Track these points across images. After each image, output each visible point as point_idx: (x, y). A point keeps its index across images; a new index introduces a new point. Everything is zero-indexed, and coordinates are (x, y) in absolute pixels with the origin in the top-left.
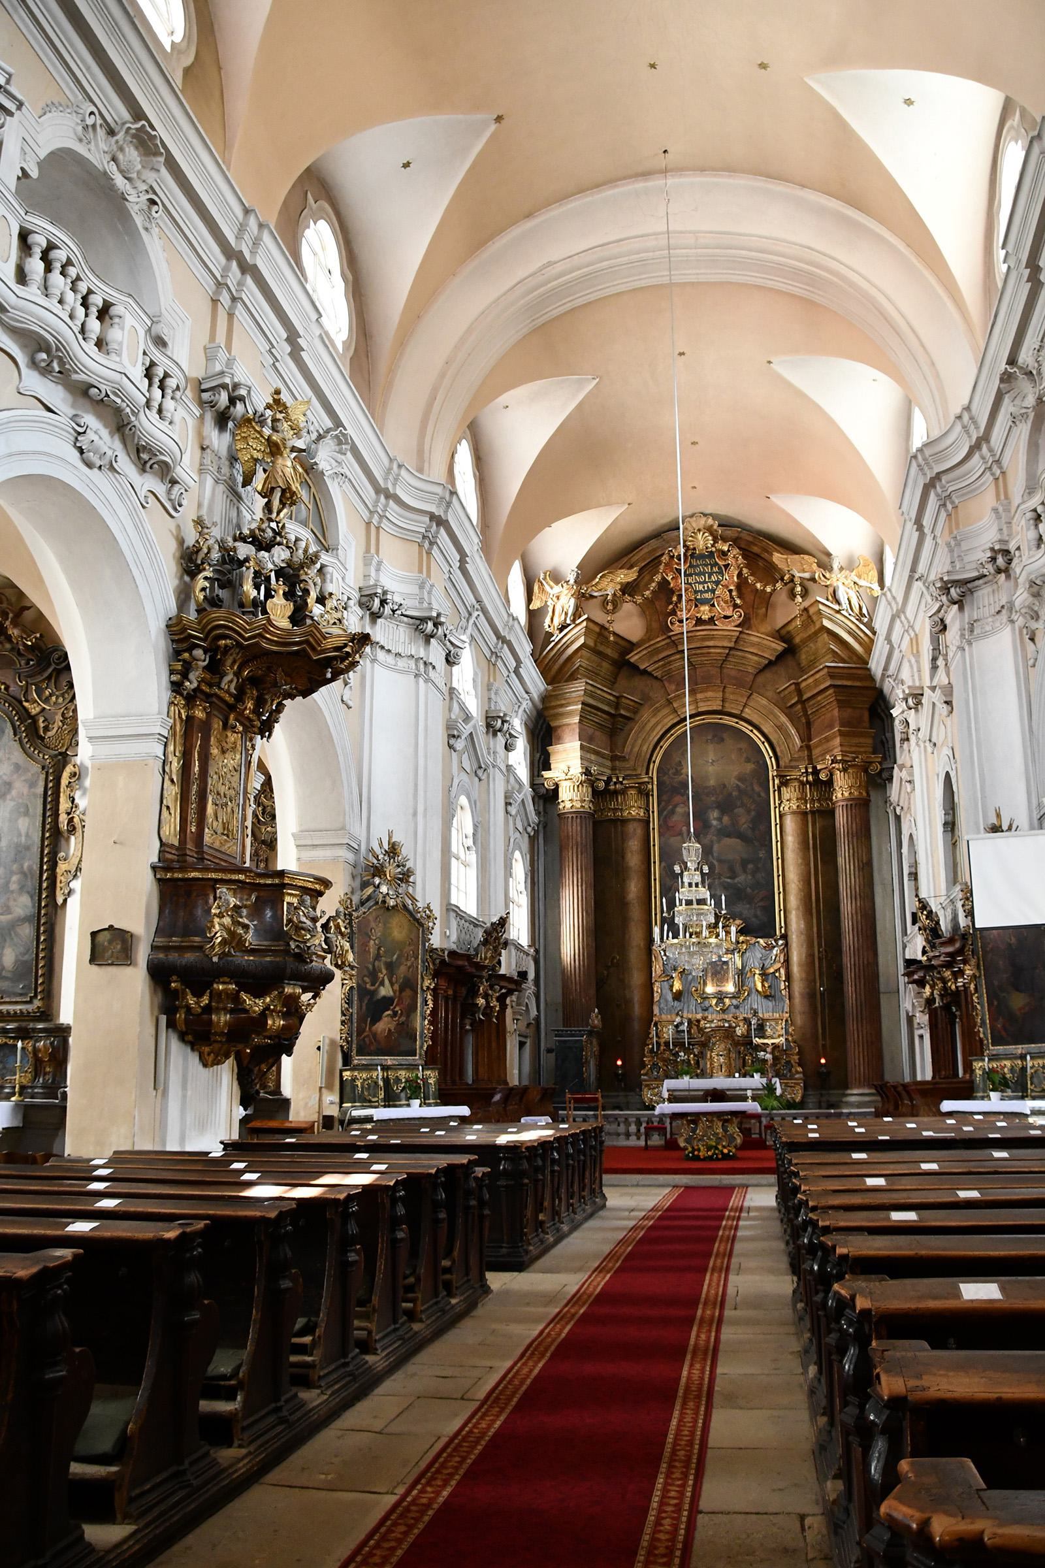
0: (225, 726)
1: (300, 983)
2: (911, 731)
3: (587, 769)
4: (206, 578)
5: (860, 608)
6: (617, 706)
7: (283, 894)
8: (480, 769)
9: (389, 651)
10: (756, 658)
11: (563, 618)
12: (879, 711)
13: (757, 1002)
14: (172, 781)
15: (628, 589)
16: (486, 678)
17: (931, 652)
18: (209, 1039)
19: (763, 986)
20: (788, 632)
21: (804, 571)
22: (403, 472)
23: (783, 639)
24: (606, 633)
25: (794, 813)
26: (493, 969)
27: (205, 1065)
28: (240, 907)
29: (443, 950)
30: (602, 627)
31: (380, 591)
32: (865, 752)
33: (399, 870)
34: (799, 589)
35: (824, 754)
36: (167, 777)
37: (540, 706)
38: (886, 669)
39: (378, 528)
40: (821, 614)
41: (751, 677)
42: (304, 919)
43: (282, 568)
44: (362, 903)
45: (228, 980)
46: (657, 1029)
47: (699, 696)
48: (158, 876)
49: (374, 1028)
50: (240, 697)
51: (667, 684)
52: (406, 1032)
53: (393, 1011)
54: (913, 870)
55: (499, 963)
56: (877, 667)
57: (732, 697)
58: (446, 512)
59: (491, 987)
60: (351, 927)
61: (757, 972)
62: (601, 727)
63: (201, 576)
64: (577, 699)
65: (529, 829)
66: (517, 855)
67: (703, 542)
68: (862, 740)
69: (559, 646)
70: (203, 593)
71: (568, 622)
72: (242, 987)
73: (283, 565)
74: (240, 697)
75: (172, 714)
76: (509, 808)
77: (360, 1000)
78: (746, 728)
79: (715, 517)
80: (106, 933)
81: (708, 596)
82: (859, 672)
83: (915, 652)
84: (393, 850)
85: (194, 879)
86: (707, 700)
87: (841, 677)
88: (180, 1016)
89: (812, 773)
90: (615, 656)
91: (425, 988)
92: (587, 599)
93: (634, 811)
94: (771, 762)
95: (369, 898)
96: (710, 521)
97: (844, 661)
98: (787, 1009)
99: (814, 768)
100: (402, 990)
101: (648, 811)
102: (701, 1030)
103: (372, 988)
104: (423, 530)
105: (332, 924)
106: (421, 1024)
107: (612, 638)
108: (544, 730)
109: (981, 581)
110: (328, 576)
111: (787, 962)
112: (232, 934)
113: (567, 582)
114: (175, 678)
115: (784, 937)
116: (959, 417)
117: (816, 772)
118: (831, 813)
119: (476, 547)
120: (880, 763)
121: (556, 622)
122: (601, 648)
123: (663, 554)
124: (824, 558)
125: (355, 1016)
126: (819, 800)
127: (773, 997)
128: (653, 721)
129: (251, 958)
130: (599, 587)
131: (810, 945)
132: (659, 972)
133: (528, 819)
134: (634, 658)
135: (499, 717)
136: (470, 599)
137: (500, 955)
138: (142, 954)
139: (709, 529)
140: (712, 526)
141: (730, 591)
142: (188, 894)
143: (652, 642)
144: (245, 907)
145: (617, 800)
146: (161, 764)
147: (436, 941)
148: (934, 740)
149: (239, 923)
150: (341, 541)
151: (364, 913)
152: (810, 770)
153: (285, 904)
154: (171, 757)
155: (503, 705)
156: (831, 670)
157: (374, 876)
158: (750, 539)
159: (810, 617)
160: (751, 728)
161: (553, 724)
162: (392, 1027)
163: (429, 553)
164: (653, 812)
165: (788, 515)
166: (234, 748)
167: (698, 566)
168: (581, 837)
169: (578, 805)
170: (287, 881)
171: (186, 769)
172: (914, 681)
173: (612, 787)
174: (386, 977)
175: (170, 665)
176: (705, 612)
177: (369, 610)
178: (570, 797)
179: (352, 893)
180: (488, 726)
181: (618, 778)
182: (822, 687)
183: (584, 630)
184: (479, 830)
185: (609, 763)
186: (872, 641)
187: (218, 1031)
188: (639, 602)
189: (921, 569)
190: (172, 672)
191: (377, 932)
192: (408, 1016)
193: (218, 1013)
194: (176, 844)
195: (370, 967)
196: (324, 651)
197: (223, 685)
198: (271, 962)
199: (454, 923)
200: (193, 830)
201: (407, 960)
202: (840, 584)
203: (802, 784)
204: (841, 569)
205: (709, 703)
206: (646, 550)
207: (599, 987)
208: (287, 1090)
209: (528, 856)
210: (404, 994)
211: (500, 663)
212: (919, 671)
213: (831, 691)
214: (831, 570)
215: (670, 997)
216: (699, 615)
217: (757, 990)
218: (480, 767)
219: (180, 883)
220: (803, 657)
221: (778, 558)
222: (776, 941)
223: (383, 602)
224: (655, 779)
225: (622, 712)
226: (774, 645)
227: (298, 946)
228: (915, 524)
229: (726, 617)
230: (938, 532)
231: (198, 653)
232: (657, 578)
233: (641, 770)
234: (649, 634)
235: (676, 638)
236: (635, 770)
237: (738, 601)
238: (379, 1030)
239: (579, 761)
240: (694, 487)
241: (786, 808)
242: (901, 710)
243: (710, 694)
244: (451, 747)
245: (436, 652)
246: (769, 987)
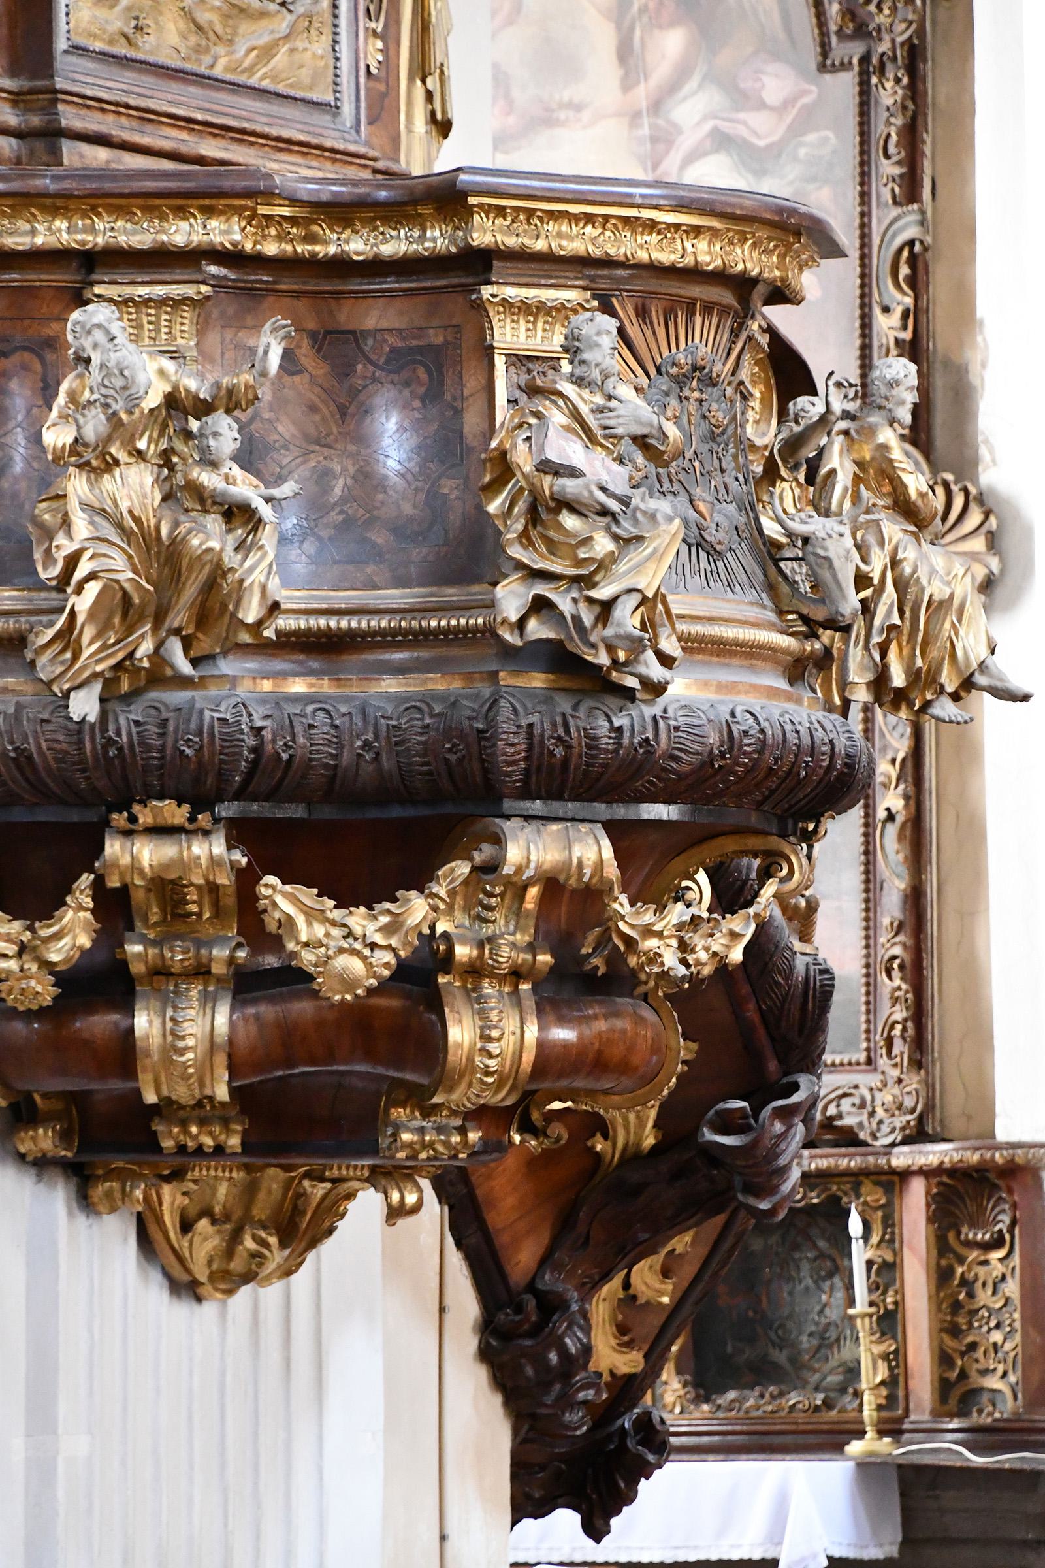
1: (602, 810)
129: (298, 686)
144: (232, 402)
149: (204, 499)
153: (500, 362)
187: (183, 1093)
193: (170, 1001)
198: (412, 705)
227: (540, 605)
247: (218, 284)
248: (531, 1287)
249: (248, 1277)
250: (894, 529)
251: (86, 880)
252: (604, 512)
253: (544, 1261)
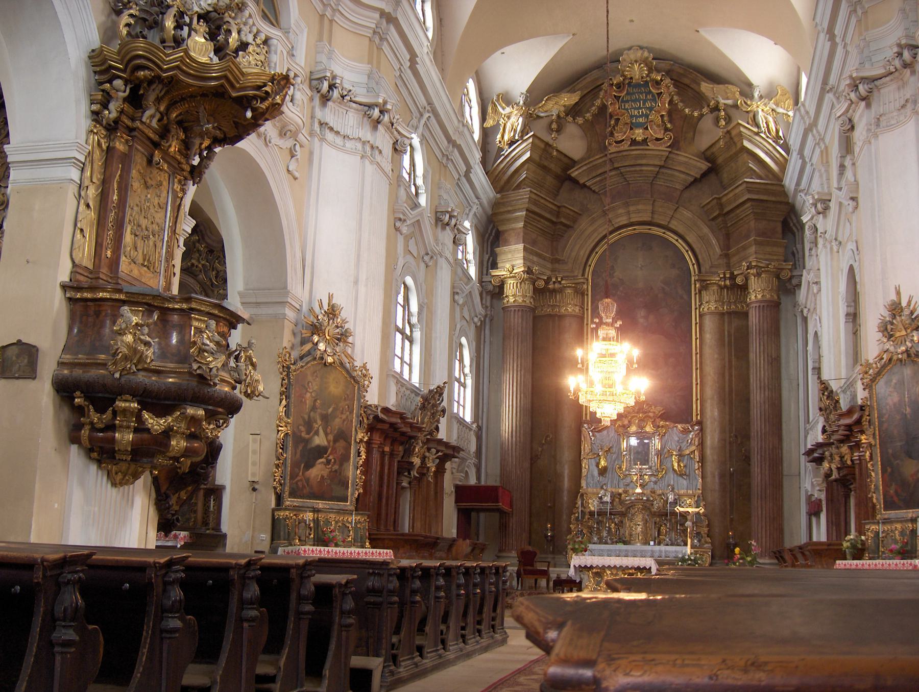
0: (150, 162)
1: (203, 406)
2: (819, 234)
3: (529, 268)
4: (131, 16)
5: (777, 131)
6: (558, 215)
7: (190, 318)
8: (428, 258)
9: (337, 133)
10: (682, 176)
11: (512, 134)
12: (792, 224)
13: (671, 478)
14: (88, 206)
15: (574, 111)
16: (437, 177)
17: (839, 159)
18: (114, 458)
19: (679, 465)
20: (713, 153)
21: (728, 99)
23: (707, 159)
24: (550, 150)
25: (712, 313)
26: (431, 433)
27: (114, 485)
28: (142, 326)
29: (376, 407)
30: (547, 144)
31: (328, 74)
32: (778, 260)
33: (338, 330)
34: (723, 113)
35: (741, 261)
36: (82, 201)
37: (490, 212)
38: (798, 184)
39: (331, 21)
40: (741, 135)
41: (678, 193)
42: (208, 342)
43: (209, 12)
44: (301, 358)
45: (130, 398)
46: (583, 500)
47: (632, 208)
48: (68, 295)
49: (308, 473)
50: (164, 133)
51: (603, 197)
53: (327, 460)
54: (817, 365)
55: (437, 429)
56: (791, 181)
57: (660, 210)
58: (395, 10)
59: (429, 449)
60: (289, 378)
61: (675, 453)
63: (127, 12)
64: (522, 206)
65: (476, 320)
66: (464, 340)
67: (637, 72)
68: (775, 249)
69: (508, 159)
70: (127, 28)
71: (517, 138)
72: (144, 406)
73: (210, 9)
74: (164, 133)
75: (91, 141)
76: (456, 297)
77: (295, 446)
78: (672, 238)
79: (650, 50)
80: (14, 347)
81: (641, 120)
82: (774, 188)
83: (825, 162)
84: (332, 312)
85: (102, 300)
86: (639, 211)
87: (758, 192)
88: (85, 433)
89: (730, 278)
90: (559, 171)
91: (358, 440)
92: (535, 119)
94: (693, 269)
95: (309, 353)
96: (646, 54)
97: (761, 179)
98: (699, 486)
99: (732, 273)
100: (335, 441)
101: (583, 309)
102: (621, 502)
103: (307, 436)
104: (374, 26)
105: (242, 354)
106: (353, 473)
107: (555, 153)
108: (493, 234)
109: (888, 79)
110: (273, 48)
111: (702, 444)
112: (135, 351)
113: (517, 104)
114: (95, 107)
115: (700, 423)
117: (733, 277)
118: (746, 315)
119: (425, 50)
120: (791, 270)
121: (506, 138)
122: (546, 163)
123: (603, 84)
124: (746, 89)
125: (289, 462)
126: (735, 303)
127: (689, 476)
128: (591, 229)
130: (545, 109)
131: (722, 431)
132: (587, 450)
133: (475, 310)
134: (574, 173)
135: (448, 212)
136: (422, 101)
137: (438, 421)
138: (48, 368)
139: (645, 61)
140: (647, 58)
141: (662, 116)
142: (97, 314)
143: (591, 160)
145: (556, 297)
146: (76, 189)
147: (372, 397)
148: (840, 239)
150: (292, 26)
151: (302, 367)
152: (728, 276)
154: (87, 182)
155: (452, 202)
156: (749, 185)
157: (313, 334)
158: (682, 71)
159: (731, 138)
160: (676, 238)
161: (501, 228)
162: (325, 473)
163: (379, 49)
164: (587, 310)
165: (715, 49)
166: (160, 184)
167: (634, 93)
168: (522, 327)
169: (520, 300)
170: (194, 305)
171: (103, 196)
172: (823, 188)
173: (551, 286)
174: (320, 428)
175: (91, 95)
176: (639, 134)
177: (318, 92)
178: (513, 293)
179: (292, 348)
180: (438, 220)
181: (557, 278)
182: (741, 200)
183: (530, 146)
184: (425, 310)
185: (549, 265)
186: (786, 160)
187: (122, 448)
188: (580, 122)
189: (832, 80)
190: (92, 102)
191: (314, 386)
192: (341, 465)
194: (91, 267)
195: (306, 417)
196: (244, 88)
197: (144, 119)
199: (393, 389)
200: (109, 256)
201: (342, 413)
202: (760, 110)
203: (721, 288)
204: (761, 97)
205: (640, 215)
206: (589, 80)
207: (534, 459)
208: (225, 528)
209: (474, 343)
210: (337, 444)
211: (450, 166)
212: (828, 179)
213: (748, 205)
214: (752, 97)
215: (596, 473)
216: (633, 137)
217: (674, 470)
218: (427, 254)
219: (89, 303)
220: (725, 175)
221: (705, 87)
222: (692, 426)
223: (332, 87)
224: (590, 280)
225: (563, 220)
226: (699, 164)
227: (199, 368)
228: (827, 33)
229: (657, 139)
230: (848, 40)
231: (118, 83)
232: (598, 102)
233: (578, 273)
234: (590, 152)
235: (612, 156)
236: (572, 271)
237: (669, 126)
238: (312, 476)
239: (522, 261)
240: (632, 21)
241: (706, 309)
242: (809, 218)
243: (640, 207)
244: (397, 229)
245: (383, 140)
246: (685, 466)
247: (146, 309)
248: (165, 493)
249: (126, 484)
250: (250, 368)
251: (111, 408)
252: (212, 353)
253: (167, 489)
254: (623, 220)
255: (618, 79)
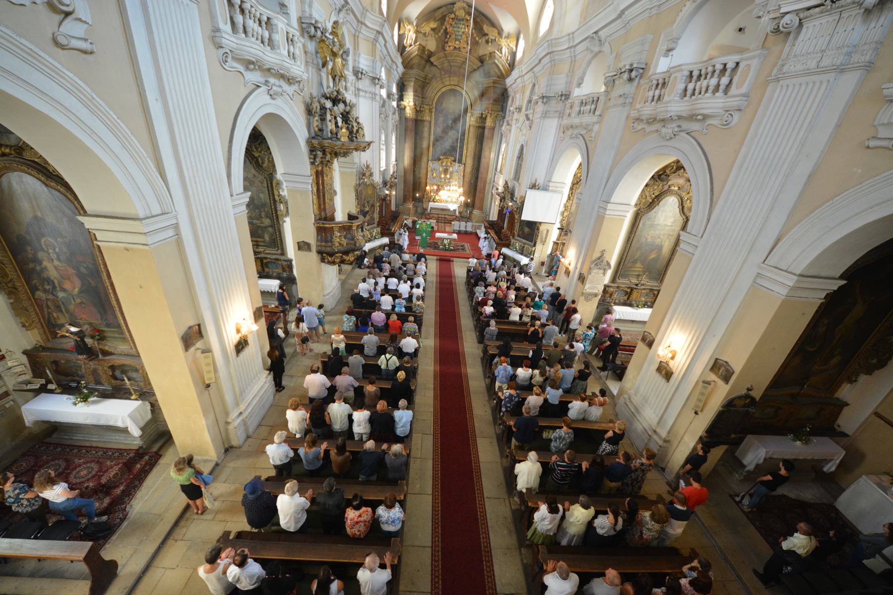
6: (425, 79)
15: (433, 30)
22: (368, 14)
52: (372, 219)
62: (419, 86)
81: (459, 37)
84: (368, 167)
86: (453, 80)
93: (427, 118)
114: (312, 160)
116: (569, 35)
134: (432, 59)
138: (314, 248)
139: (464, 8)
178: (409, 112)
190: (310, 158)
191: (364, 193)
221: (486, 28)
232: (444, 27)
254: (448, 83)
255: (453, 16)
